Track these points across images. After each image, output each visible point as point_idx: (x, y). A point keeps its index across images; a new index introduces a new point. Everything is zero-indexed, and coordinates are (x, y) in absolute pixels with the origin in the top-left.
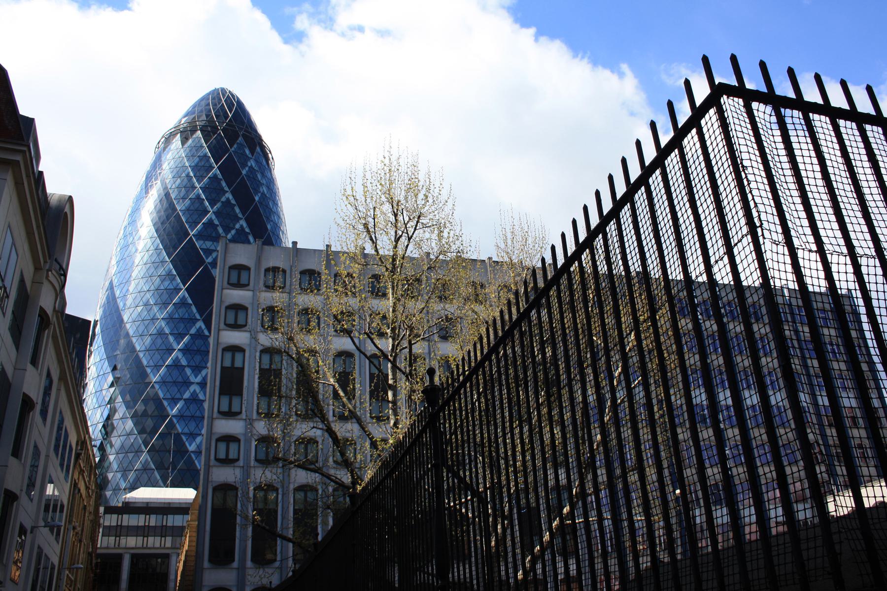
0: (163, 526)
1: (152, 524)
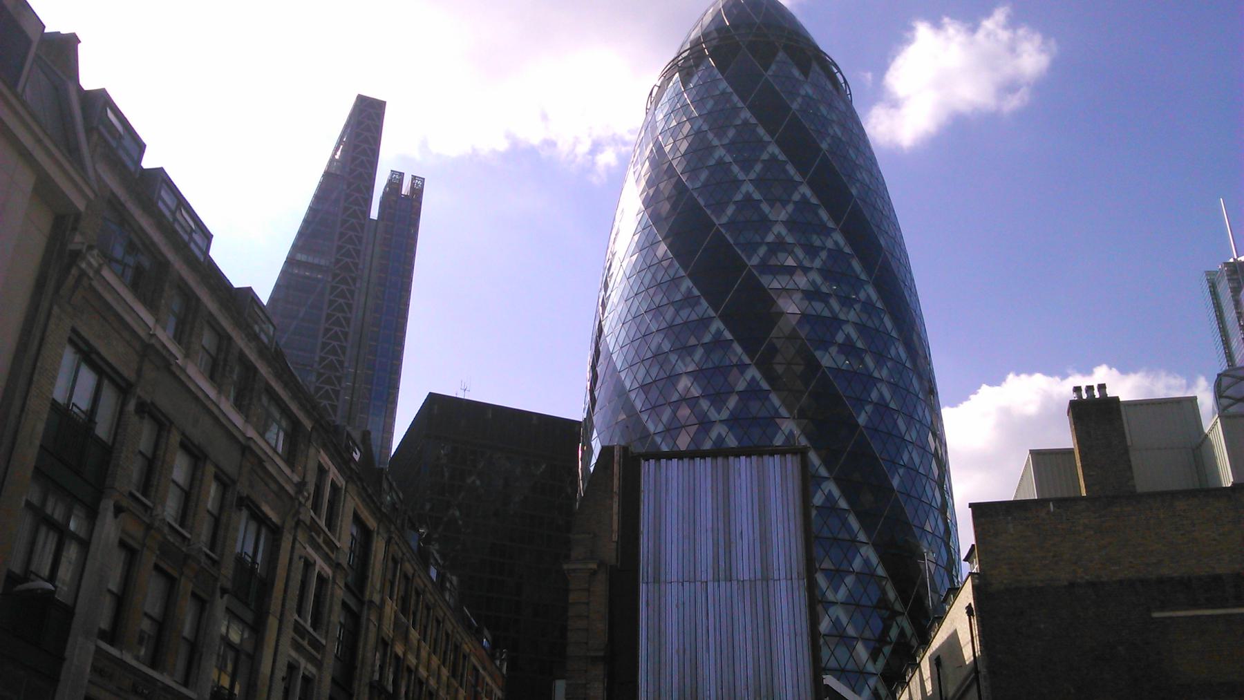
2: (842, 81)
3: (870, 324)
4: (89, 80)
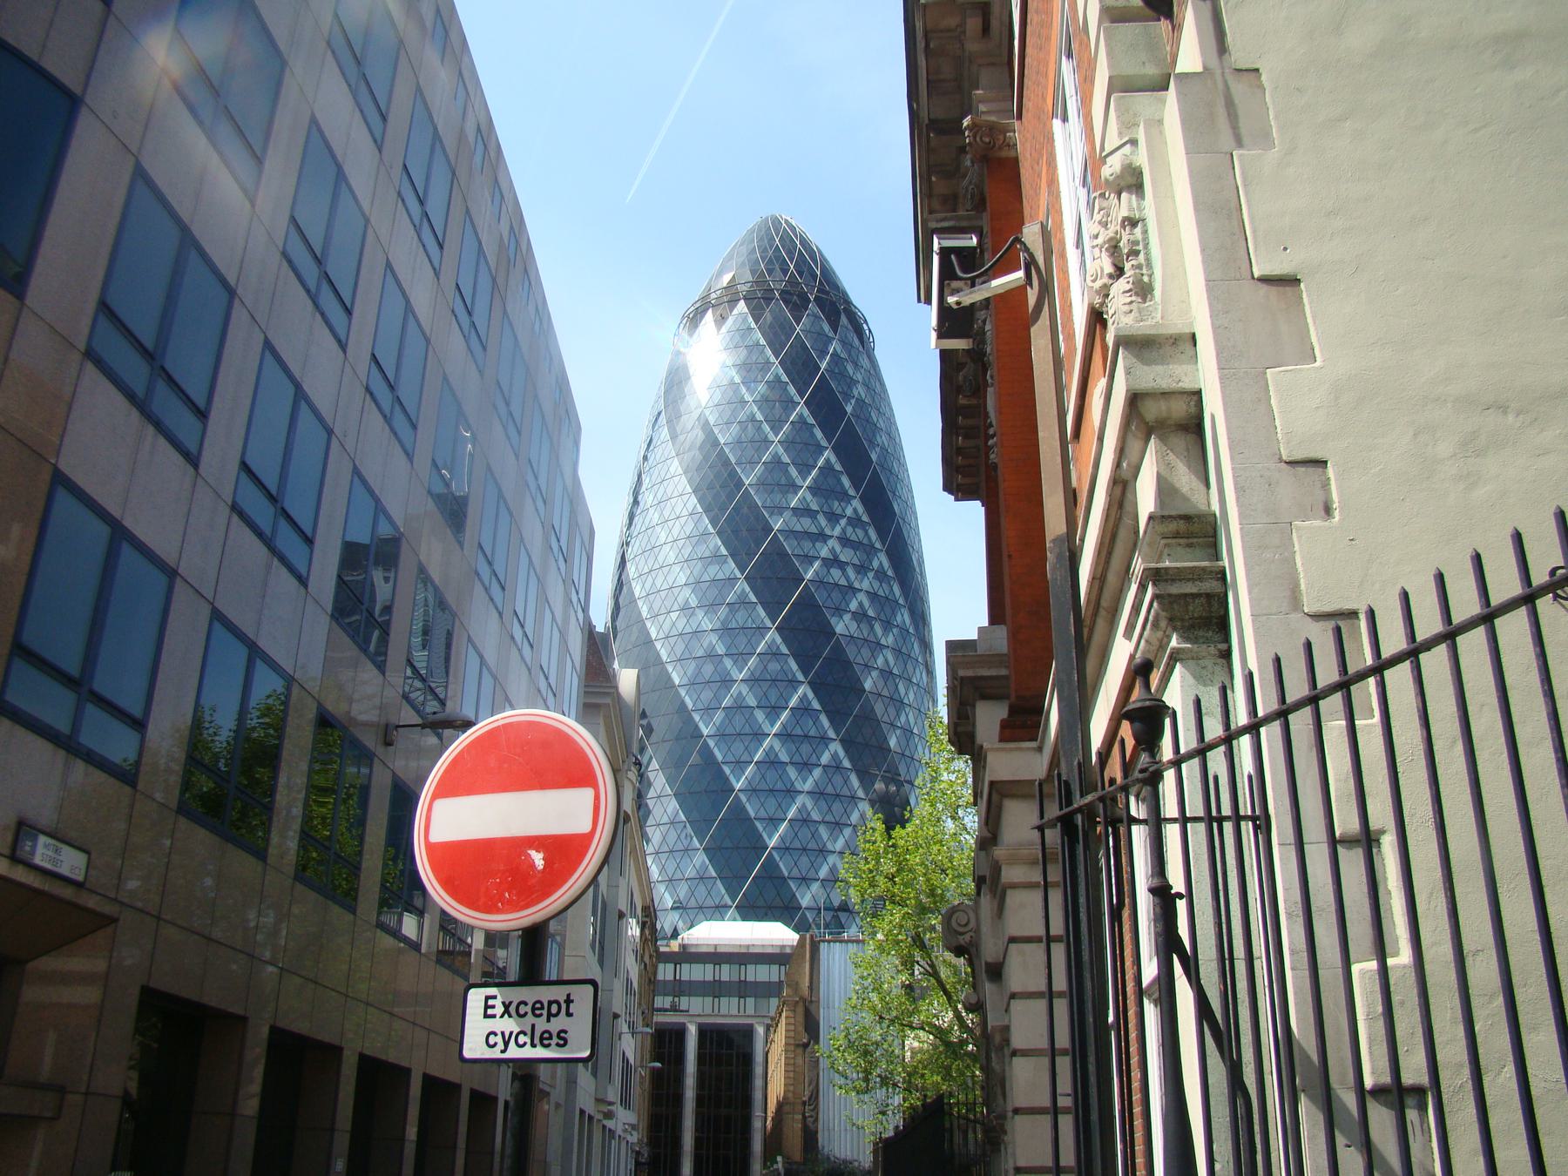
0: (740, 981)
1: (725, 977)
3: (881, 593)
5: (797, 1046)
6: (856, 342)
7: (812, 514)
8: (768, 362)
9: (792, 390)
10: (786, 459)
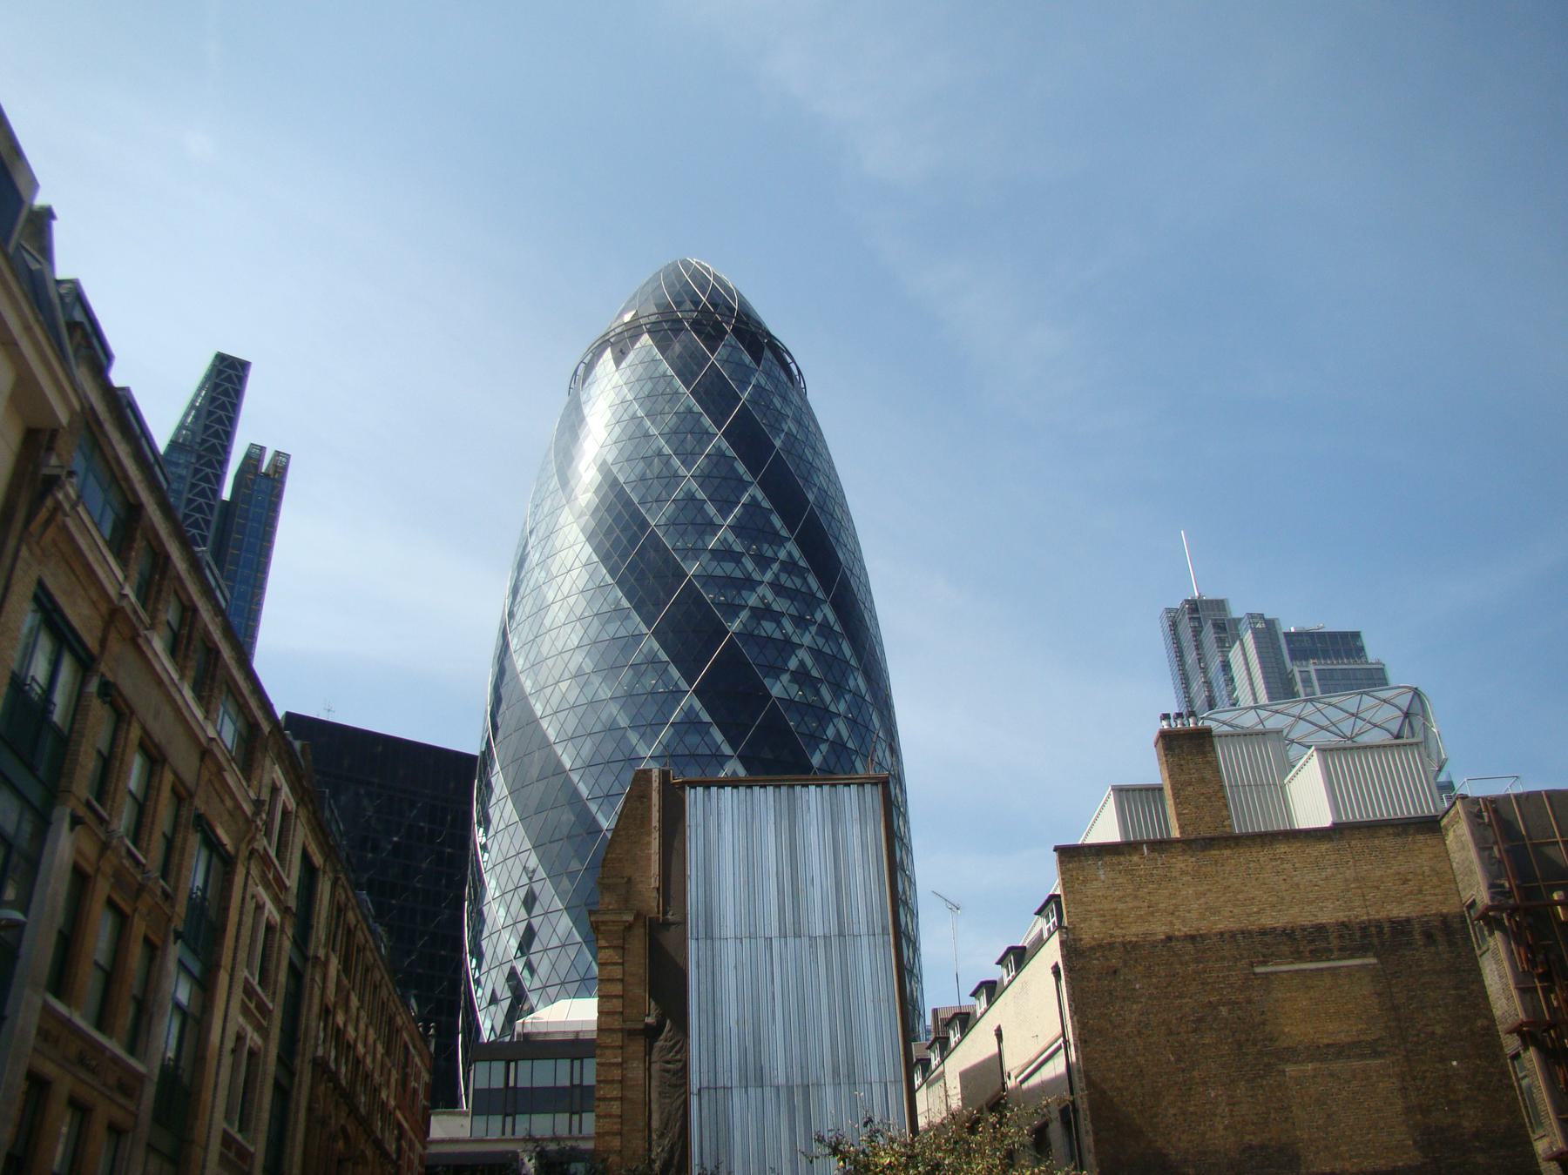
2: (796, 372)
3: (827, 650)
4: (64, 268)
5: (630, 1034)
6: (784, 377)
7: (736, 558)
8: (676, 393)
9: (707, 421)
10: (701, 495)
